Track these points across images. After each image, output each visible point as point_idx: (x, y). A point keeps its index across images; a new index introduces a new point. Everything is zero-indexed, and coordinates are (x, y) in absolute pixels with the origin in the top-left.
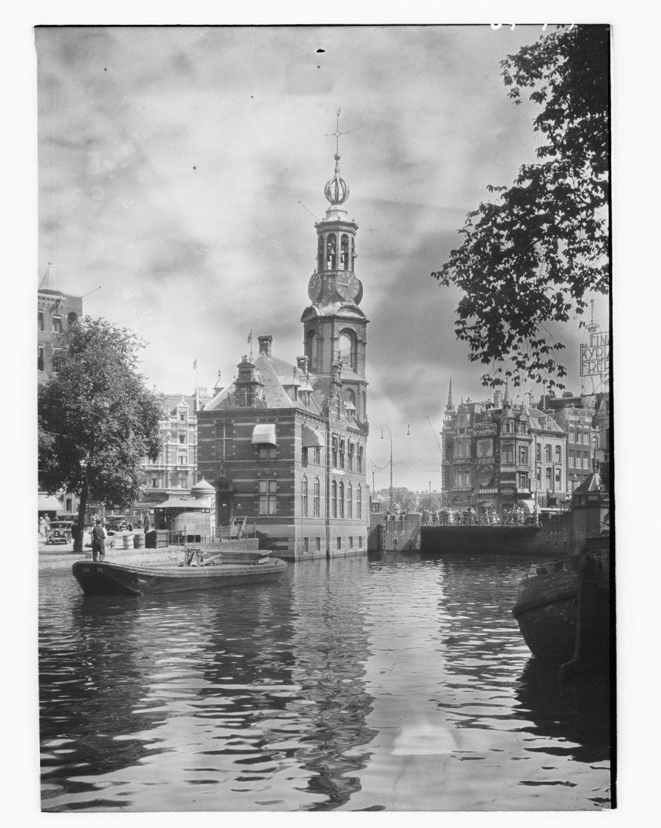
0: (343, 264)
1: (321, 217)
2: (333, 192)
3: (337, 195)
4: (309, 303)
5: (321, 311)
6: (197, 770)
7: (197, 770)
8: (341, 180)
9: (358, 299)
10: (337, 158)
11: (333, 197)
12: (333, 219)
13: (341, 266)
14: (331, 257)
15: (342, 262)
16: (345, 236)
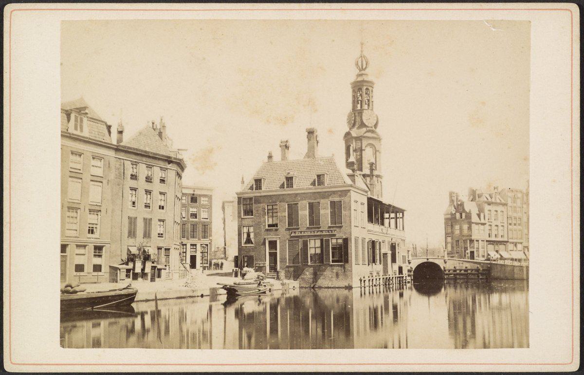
0: (367, 105)
1: (353, 78)
2: (360, 64)
3: (362, 67)
4: (347, 130)
5: (355, 133)
6: (166, 299)
7: (166, 299)
8: (364, 57)
9: (376, 126)
10: (362, 44)
11: (360, 66)
12: (360, 79)
13: (366, 107)
14: (359, 102)
15: (366, 104)
16: (367, 89)
